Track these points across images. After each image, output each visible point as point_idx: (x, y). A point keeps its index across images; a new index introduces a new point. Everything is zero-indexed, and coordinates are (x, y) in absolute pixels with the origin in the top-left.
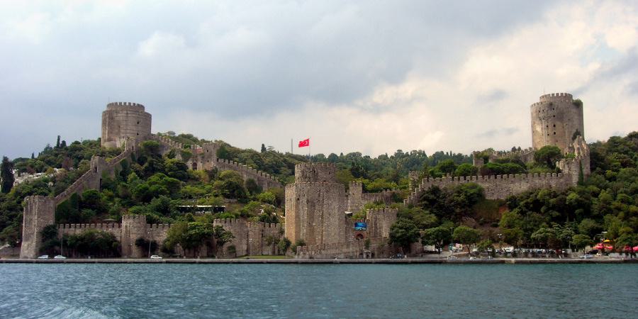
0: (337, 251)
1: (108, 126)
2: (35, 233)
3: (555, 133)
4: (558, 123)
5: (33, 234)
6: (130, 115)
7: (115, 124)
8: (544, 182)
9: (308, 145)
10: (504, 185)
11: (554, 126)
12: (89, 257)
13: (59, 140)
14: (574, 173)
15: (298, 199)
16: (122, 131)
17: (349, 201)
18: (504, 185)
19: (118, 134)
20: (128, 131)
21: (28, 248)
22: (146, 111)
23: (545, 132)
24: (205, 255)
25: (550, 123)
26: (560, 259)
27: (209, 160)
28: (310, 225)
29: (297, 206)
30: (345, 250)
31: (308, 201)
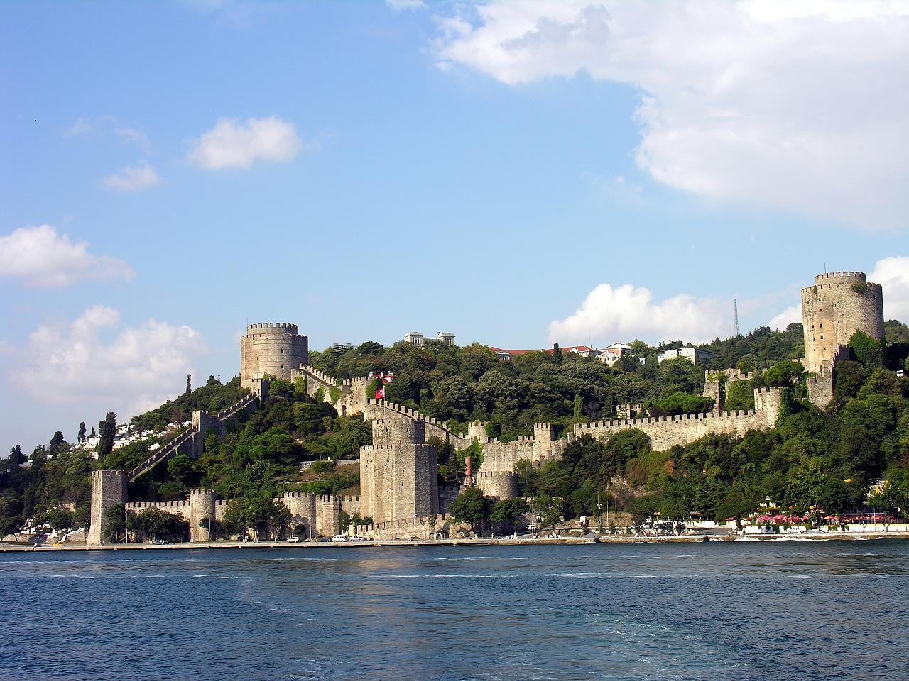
0: (401, 530)
2: (100, 515)
3: (822, 336)
4: (826, 321)
7: (253, 355)
8: (727, 425)
11: (821, 326)
13: (189, 380)
14: (769, 408)
16: (261, 364)
17: (534, 453)
20: (269, 364)
21: (94, 537)
25: (816, 321)
26: (514, 538)
30: (411, 529)
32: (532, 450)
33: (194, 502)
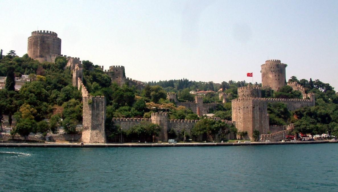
1: (40, 47)
2: (103, 125)
4: (280, 74)
5: (101, 125)
6: (55, 41)
9: (252, 76)
10: (293, 104)
11: (279, 75)
12: (146, 142)
15: (254, 107)
16: (51, 51)
18: (293, 104)
19: (48, 53)
22: (58, 37)
23: (274, 78)
24: (201, 140)
25: (277, 74)
27: (118, 77)
28: (261, 123)
29: (253, 111)
31: (259, 109)
32: (196, 106)
33: (162, 120)
